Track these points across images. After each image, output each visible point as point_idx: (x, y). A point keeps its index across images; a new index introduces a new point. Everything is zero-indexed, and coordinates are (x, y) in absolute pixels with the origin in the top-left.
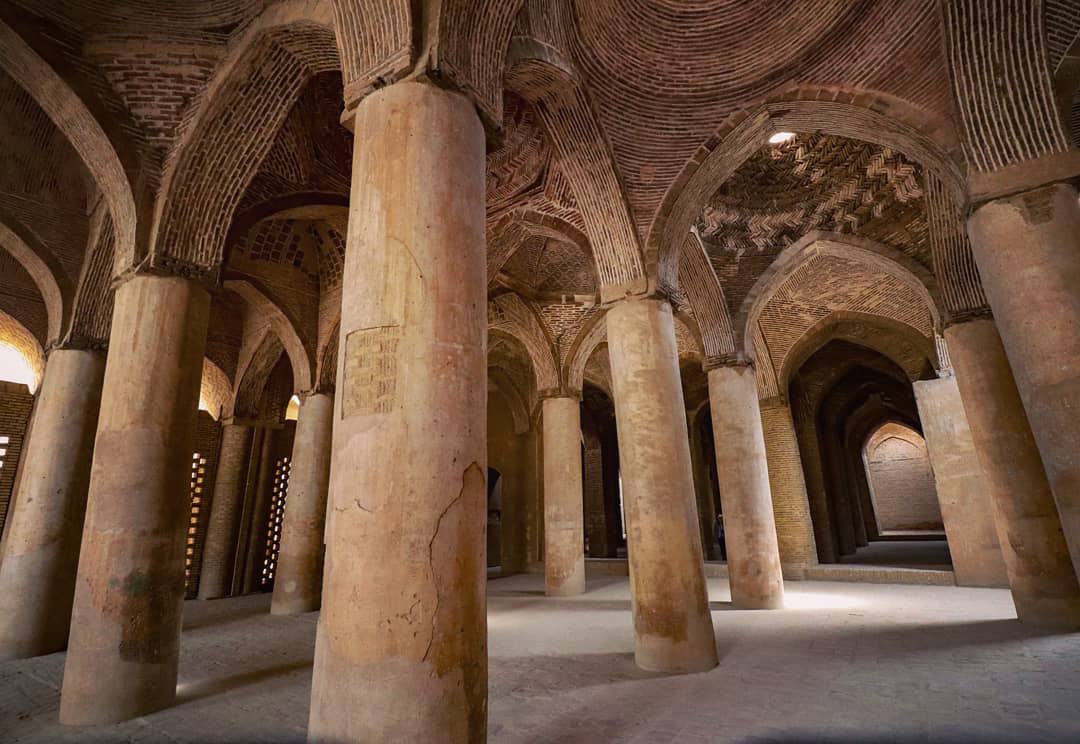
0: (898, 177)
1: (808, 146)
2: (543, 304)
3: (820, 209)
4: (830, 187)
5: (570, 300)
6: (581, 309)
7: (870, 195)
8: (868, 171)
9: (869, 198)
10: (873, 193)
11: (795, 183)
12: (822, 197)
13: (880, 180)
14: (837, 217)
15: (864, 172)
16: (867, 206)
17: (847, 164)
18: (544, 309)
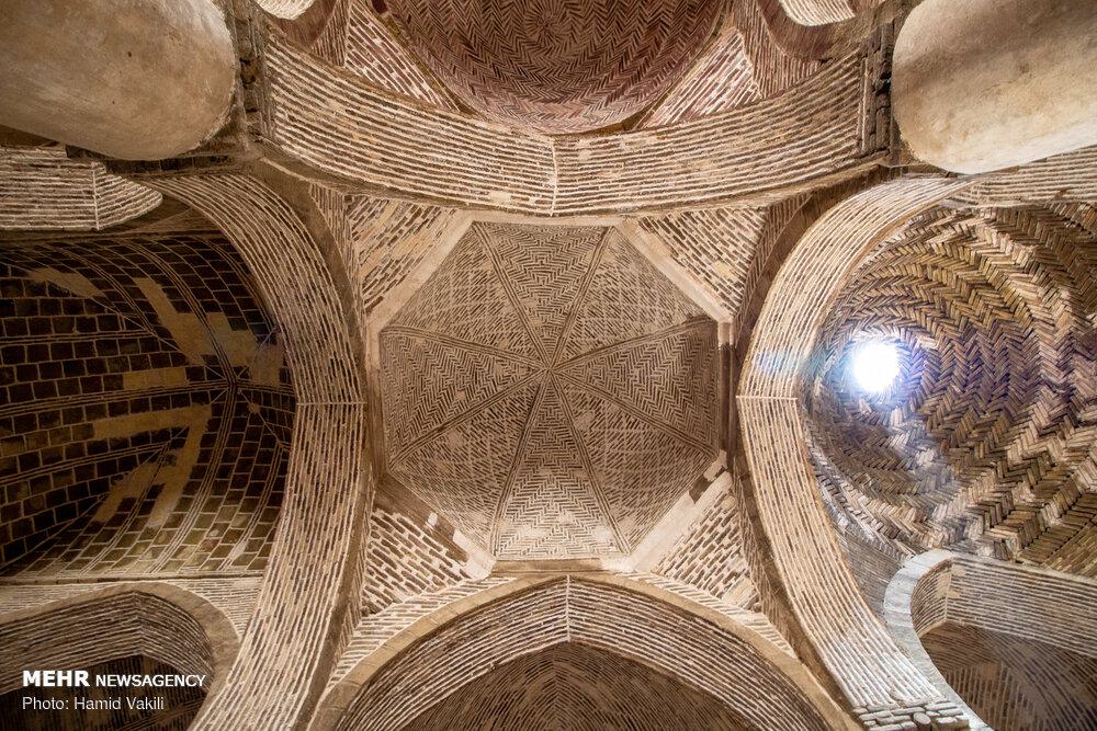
0: (1073, 450)
1: (909, 409)
2: (385, 500)
3: (941, 513)
4: (948, 480)
5: (443, 533)
6: (456, 568)
7: (1027, 490)
8: (1009, 454)
9: (1025, 495)
10: (1032, 488)
11: (893, 461)
12: (940, 494)
13: (1032, 461)
14: (974, 532)
15: (1002, 455)
16: (1027, 508)
17: (970, 444)
18: (379, 514)
